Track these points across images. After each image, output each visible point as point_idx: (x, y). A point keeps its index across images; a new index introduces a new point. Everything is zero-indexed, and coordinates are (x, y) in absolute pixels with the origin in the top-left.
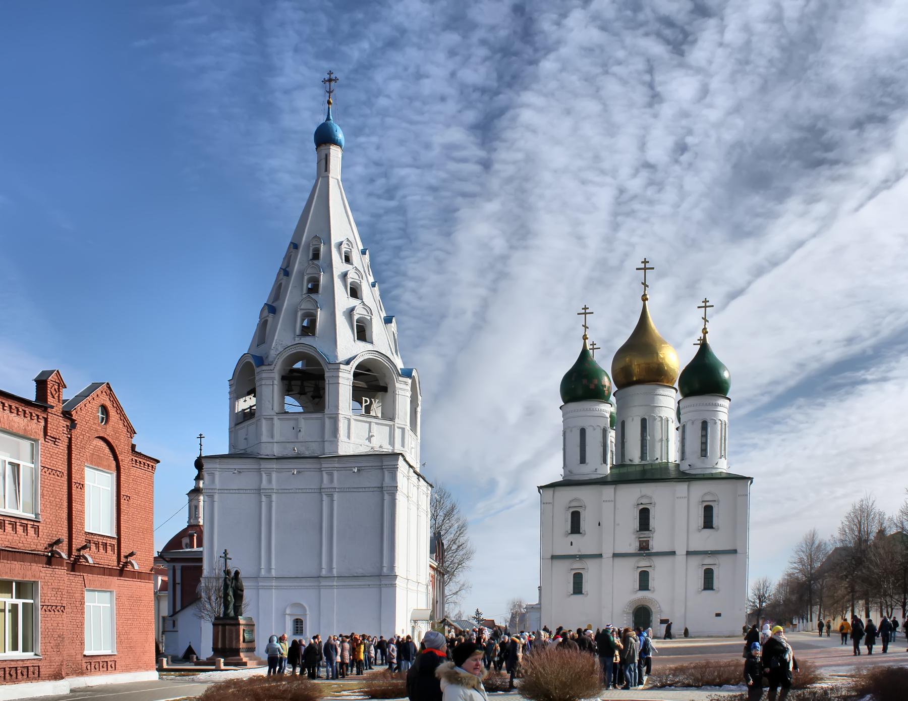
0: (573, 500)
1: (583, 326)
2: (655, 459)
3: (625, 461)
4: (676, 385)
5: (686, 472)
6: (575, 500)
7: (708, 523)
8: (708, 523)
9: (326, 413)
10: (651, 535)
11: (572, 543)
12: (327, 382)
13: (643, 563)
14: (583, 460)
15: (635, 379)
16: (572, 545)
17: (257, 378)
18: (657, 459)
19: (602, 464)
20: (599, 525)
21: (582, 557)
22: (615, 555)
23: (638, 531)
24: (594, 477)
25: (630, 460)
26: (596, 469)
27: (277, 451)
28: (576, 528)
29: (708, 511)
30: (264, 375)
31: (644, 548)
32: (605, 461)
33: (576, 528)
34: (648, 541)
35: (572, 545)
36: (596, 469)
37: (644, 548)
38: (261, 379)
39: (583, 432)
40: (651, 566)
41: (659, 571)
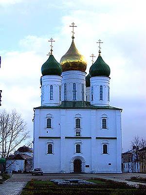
4: (87, 71)
7: (104, 127)
8: (104, 127)
13: (78, 141)
29: (104, 121)
31: (78, 137)
37: (78, 137)
41: (84, 144)
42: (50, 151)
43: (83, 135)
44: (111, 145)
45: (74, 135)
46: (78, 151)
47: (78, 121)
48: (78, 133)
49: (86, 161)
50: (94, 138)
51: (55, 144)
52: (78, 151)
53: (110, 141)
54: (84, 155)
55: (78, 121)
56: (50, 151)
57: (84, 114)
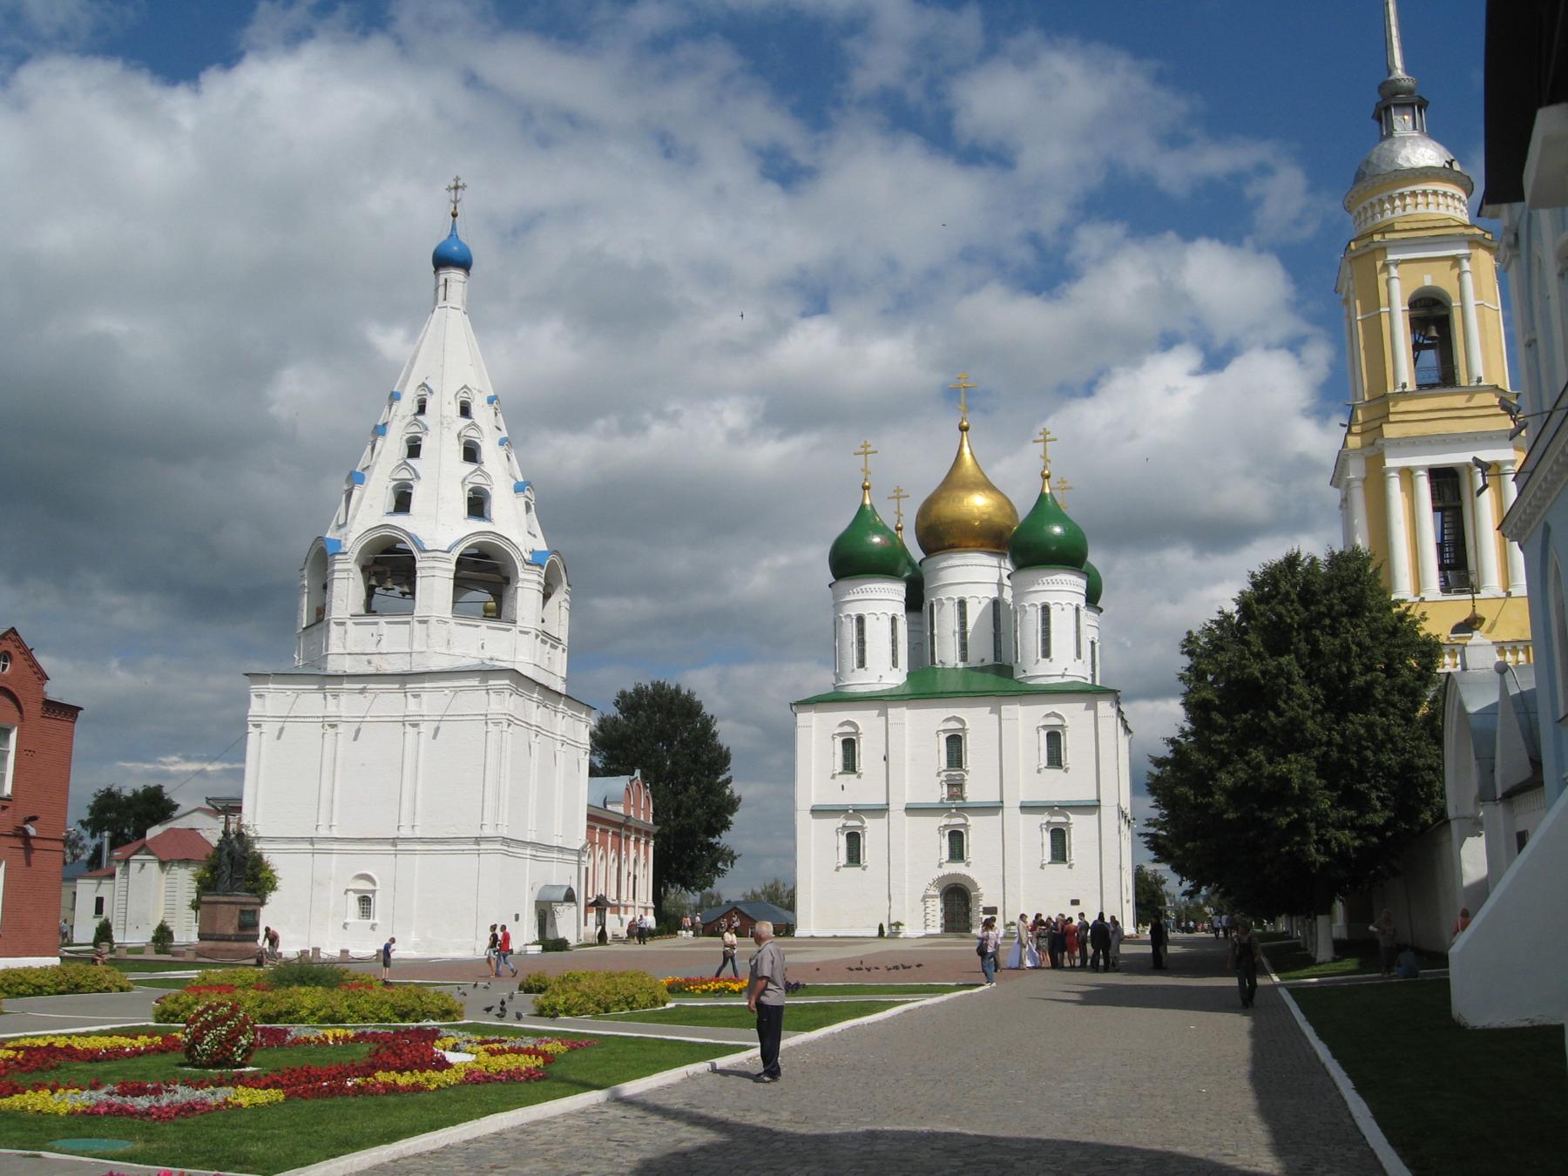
0: (842, 724)
1: (862, 470)
2: (980, 659)
3: (935, 663)
5: (1021, 681)
6: (848, 723)
9: (415, 615)
10: (966, 778)
11: (843, 787)
12: (418, 574)
14: (862, 664)
15: (947, 544)
16: (843, 789)
17: (329, 571)
18: (983, 660)
19: (891, 670)
20: (885, 759)
21: (859, 811)
22: (912, 810)
23: (944, 771)
24: (878, 688)
25: (941, 661)
26: (881, 677)
27: (349, 666)
28: (850, 765)
29: (1054, 738)
30: (337, 567)
32: (895, 664)
33: (850, 765)
34: (961, 785)
35: (843, 789)
36: (881, 677)
38: (334, 571)
39: (860, 620)
40: (965, 824)
41: (979, 831)
42: (854, 857)
43: (972, 794)
44: (1080, 829)
45: (937, 793)
46: (957, 852)
47: (955, 743)
48: (956, 787)
49: (987, 895)
50: (1012, 806)
51: (873, 831)
52: (957, 852)
53: (1074, 818)
54: (979, 870)
55: (955, 743)
56: (854, 857)
57: (977, 720)
